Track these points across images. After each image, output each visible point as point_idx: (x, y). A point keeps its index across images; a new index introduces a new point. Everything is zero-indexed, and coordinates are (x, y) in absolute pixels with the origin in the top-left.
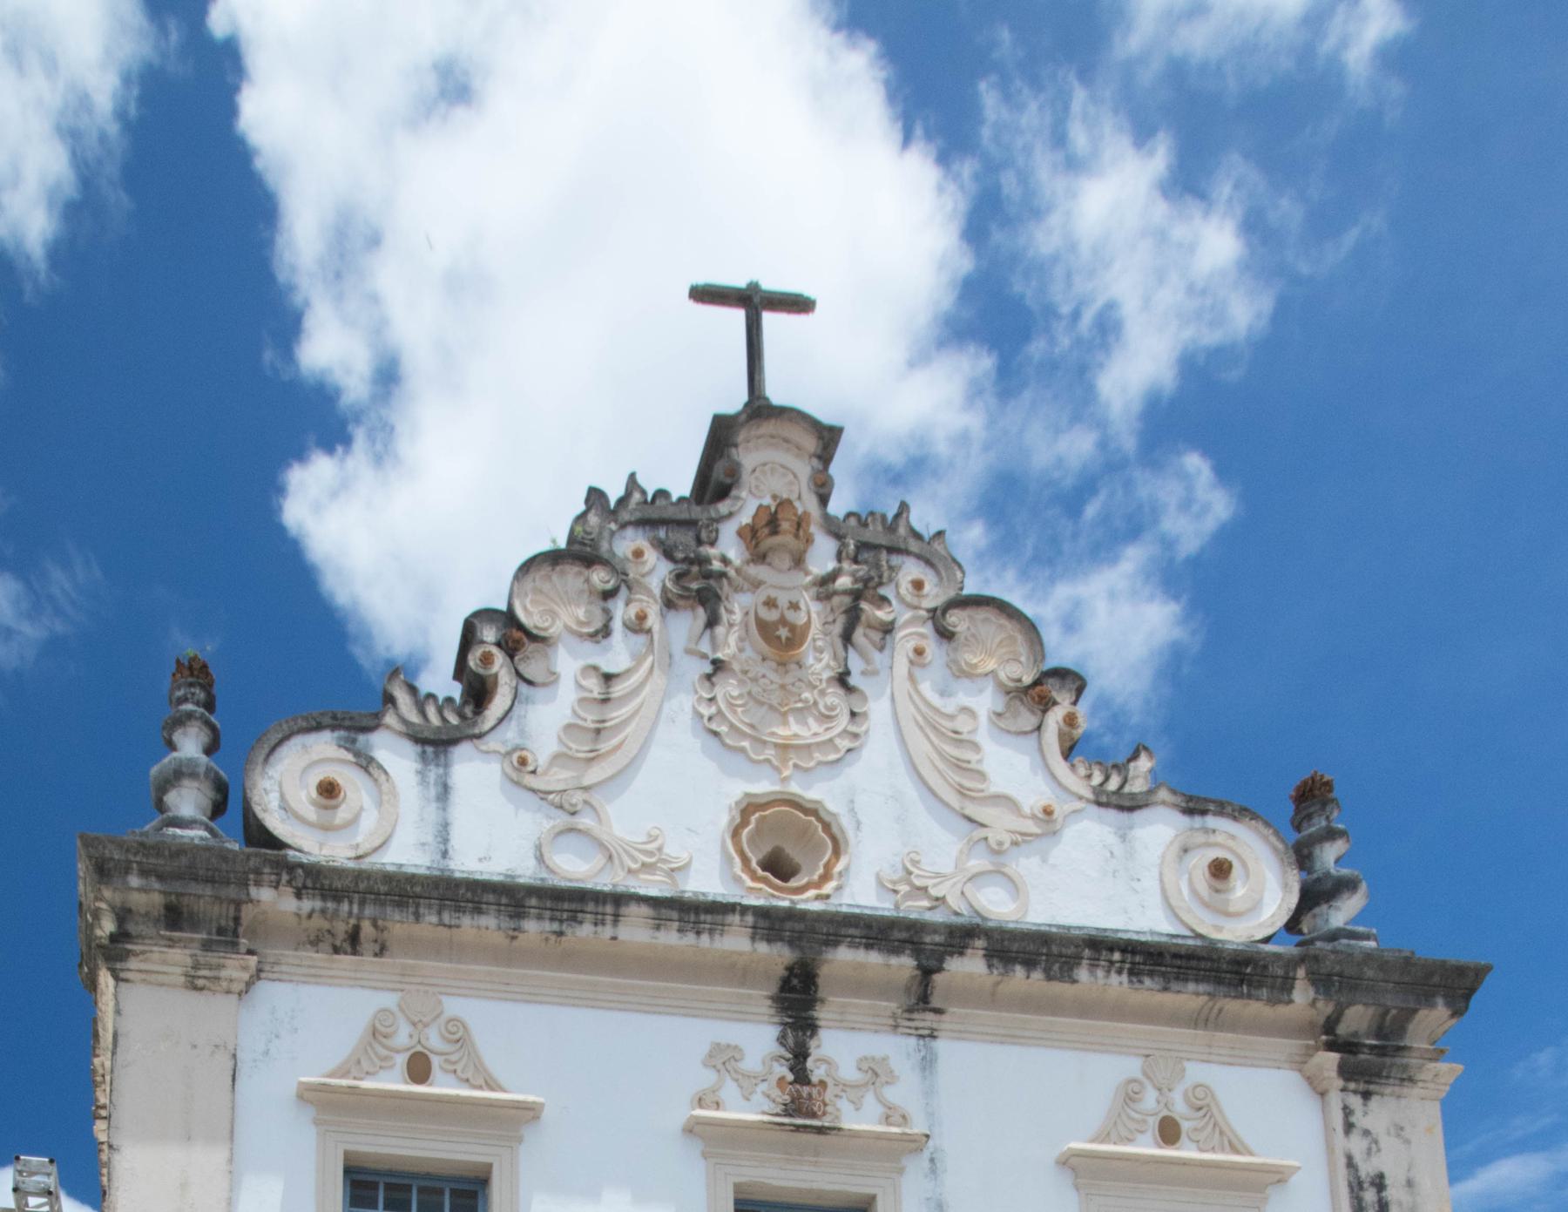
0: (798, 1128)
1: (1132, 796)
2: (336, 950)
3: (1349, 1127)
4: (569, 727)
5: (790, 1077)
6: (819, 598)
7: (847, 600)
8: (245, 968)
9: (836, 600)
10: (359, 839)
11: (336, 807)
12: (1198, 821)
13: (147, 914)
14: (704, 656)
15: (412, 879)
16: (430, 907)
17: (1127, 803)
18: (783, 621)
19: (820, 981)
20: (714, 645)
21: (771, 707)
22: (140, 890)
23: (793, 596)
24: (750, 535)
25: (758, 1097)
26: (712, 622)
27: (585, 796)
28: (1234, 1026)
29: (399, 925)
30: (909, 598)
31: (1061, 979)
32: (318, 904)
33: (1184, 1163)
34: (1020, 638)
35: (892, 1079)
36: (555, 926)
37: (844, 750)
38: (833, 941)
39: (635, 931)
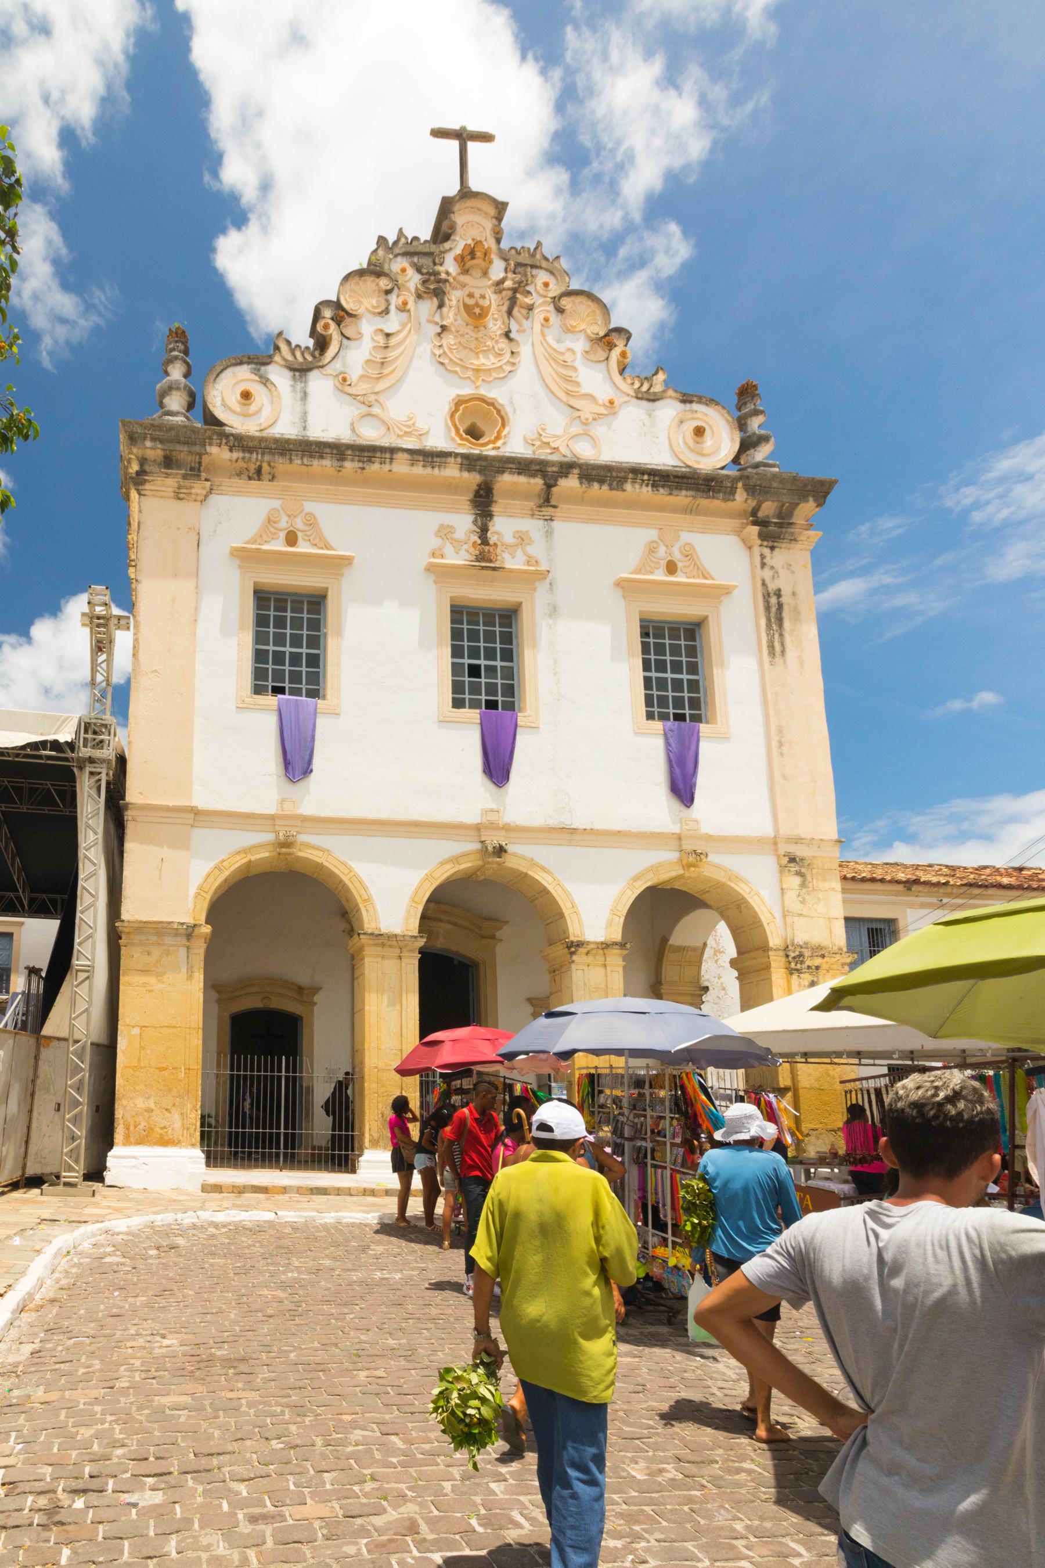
0: (483, 568)
1: (655, 393)
2: (250, 478)
3: (763, 565)
4: (368, 361)
5: (479, 541)
6: (495, 292)
7: (510, 293)
8: (204, 488)
9: (504, 293)
10: (262, 421)
11: (250, 404)
12: (688, 406)
13: (155, 461)
14: (437, 323)
15: (288, 441)
16: (297, 455)
17: (652, 398)
18: (477, 305)
19: (495, 492)
20: (442, 318)
21: (471, 349)
22: (152, 448)
23: (482, 291)
24: (461, 260)
25: (463, 552)
26: (441, 306)
27: (376, 397)
28: (706, 513)
29: (281, 464)
30: (541, 292)
31: (617, 489)
32: (241, 455)
33: (679, 584)
34: (598, 312)
35: (531, 542)
36: (361, 465)
38: (501, 471)
39: (401, 466)
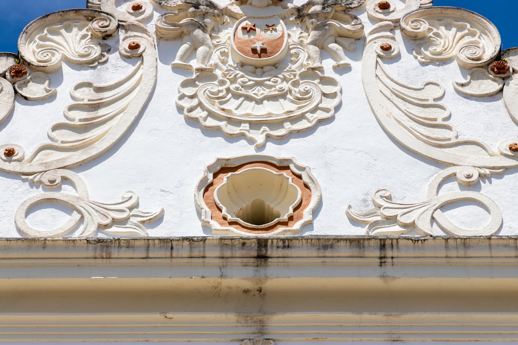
37: (316, 120)
